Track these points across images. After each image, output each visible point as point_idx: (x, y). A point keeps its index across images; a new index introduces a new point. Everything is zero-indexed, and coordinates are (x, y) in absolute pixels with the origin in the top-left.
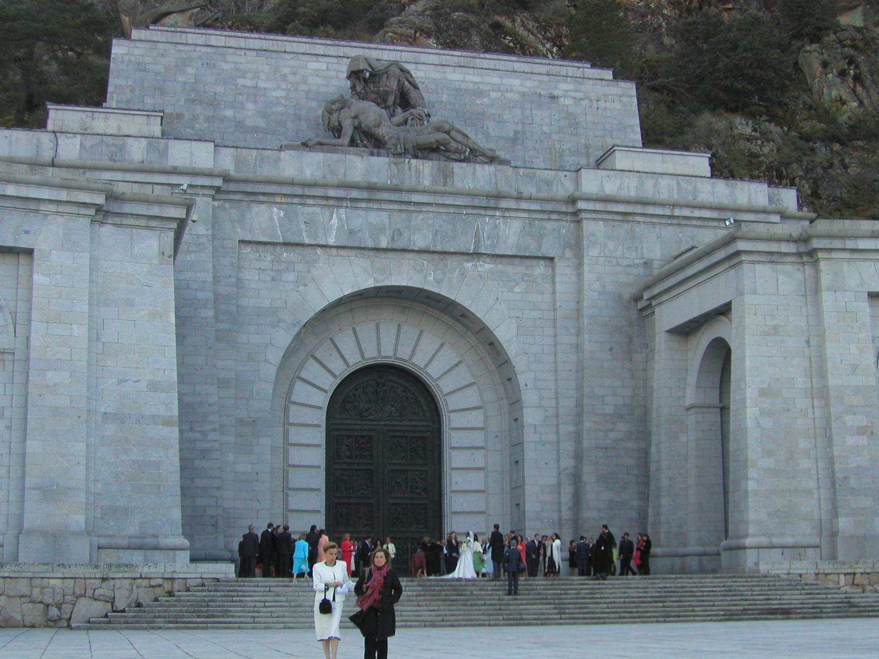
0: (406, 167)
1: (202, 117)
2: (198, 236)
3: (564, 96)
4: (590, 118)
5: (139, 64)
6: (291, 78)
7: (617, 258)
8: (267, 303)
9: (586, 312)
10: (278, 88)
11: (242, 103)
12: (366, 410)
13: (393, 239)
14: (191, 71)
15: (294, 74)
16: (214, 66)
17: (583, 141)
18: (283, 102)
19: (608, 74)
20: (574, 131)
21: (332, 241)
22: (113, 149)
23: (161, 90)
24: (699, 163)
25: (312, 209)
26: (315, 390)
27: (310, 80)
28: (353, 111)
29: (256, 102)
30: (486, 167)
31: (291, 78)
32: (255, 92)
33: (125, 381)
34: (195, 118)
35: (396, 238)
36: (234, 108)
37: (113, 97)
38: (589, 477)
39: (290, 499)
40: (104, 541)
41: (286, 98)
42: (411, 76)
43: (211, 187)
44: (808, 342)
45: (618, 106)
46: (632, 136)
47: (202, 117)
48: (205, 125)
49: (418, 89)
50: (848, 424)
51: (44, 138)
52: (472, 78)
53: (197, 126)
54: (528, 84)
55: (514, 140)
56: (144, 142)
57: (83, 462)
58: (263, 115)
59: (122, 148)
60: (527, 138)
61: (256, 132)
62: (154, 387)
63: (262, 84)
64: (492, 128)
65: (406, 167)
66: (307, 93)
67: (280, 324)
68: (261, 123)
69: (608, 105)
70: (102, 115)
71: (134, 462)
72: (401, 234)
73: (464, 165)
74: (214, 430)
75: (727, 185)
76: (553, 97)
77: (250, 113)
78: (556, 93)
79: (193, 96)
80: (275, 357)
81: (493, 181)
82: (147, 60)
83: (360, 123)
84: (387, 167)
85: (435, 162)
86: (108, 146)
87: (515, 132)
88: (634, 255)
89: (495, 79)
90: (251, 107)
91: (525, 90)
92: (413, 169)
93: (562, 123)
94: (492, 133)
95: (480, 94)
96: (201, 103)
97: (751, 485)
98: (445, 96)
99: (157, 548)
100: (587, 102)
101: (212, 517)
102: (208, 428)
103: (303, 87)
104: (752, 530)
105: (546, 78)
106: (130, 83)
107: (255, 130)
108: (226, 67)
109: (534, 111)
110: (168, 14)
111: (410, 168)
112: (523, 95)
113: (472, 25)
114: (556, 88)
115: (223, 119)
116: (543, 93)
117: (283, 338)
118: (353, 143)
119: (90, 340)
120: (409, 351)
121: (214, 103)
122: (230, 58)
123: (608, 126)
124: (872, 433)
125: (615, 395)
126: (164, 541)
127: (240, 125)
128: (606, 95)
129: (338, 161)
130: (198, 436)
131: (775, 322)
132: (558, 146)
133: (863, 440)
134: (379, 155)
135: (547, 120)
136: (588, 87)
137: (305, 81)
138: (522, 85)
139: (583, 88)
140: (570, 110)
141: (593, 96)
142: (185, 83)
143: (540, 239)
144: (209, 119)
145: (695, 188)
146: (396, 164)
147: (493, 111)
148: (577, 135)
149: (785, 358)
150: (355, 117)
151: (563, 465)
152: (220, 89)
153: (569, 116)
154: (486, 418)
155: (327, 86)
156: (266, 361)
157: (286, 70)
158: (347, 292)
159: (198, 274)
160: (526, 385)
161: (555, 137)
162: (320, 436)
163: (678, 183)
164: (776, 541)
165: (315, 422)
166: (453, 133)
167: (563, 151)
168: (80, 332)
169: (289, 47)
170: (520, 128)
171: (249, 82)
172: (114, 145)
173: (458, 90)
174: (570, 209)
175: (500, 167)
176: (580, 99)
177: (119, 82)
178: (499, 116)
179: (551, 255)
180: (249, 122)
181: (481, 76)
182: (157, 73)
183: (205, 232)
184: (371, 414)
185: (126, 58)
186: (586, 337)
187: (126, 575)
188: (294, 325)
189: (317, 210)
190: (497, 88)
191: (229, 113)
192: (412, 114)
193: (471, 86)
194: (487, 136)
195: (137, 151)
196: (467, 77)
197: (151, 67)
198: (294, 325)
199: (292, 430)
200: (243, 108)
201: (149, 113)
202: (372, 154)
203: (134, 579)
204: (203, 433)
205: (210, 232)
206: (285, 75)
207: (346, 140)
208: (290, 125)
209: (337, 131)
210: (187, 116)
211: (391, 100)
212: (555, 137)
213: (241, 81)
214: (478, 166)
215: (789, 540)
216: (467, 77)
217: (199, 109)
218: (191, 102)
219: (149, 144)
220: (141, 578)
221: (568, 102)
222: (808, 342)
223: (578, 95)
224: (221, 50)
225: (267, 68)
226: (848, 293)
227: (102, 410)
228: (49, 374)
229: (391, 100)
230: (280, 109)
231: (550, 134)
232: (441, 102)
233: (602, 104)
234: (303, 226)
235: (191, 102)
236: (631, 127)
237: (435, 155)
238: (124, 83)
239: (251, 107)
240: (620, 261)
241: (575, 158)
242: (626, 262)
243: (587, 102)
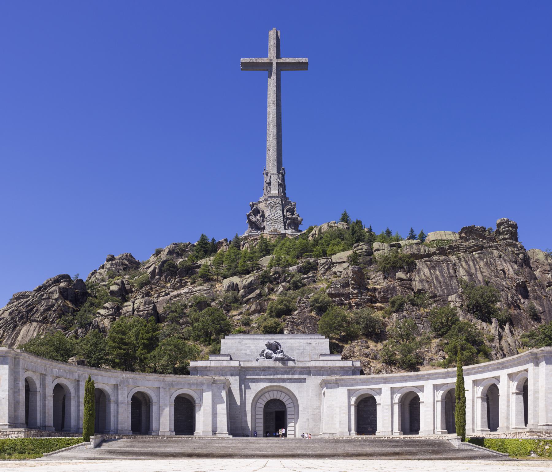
19: (324, 337)
23: (231, 348)
24: (339, 358)
28: (266, 352)
34: (237, 353)
37: (222, 352)
51: (209, 362)
55: (302, 353)
58: (251, 352)
59: (222, 363)
68: (250, 353)
76: (310, 343)
77: (248, 352)
89: (298, 341)
90: (248, 350)
93: (312, 349)
100: (318, 344)
107: (249, 355)
115: (243, 353)
121: (241, 350)
127: (246, 354)
136: (318, 341)
144: (240, 353)
150: (266, 353)
169: (256, 337)
171: (248, 346)
180: (248, 353)
189: (259, 371)
191: (244, 352)
195: (225, 364)
201: (227, 355)
209: (263, 355)
210: (236, 353)
212: (311, 352)
213: (246, 345)
217: (238, 351)
230: (254, 350)
233: (321, 344)
236: (327, 348)
239: (248, 350)
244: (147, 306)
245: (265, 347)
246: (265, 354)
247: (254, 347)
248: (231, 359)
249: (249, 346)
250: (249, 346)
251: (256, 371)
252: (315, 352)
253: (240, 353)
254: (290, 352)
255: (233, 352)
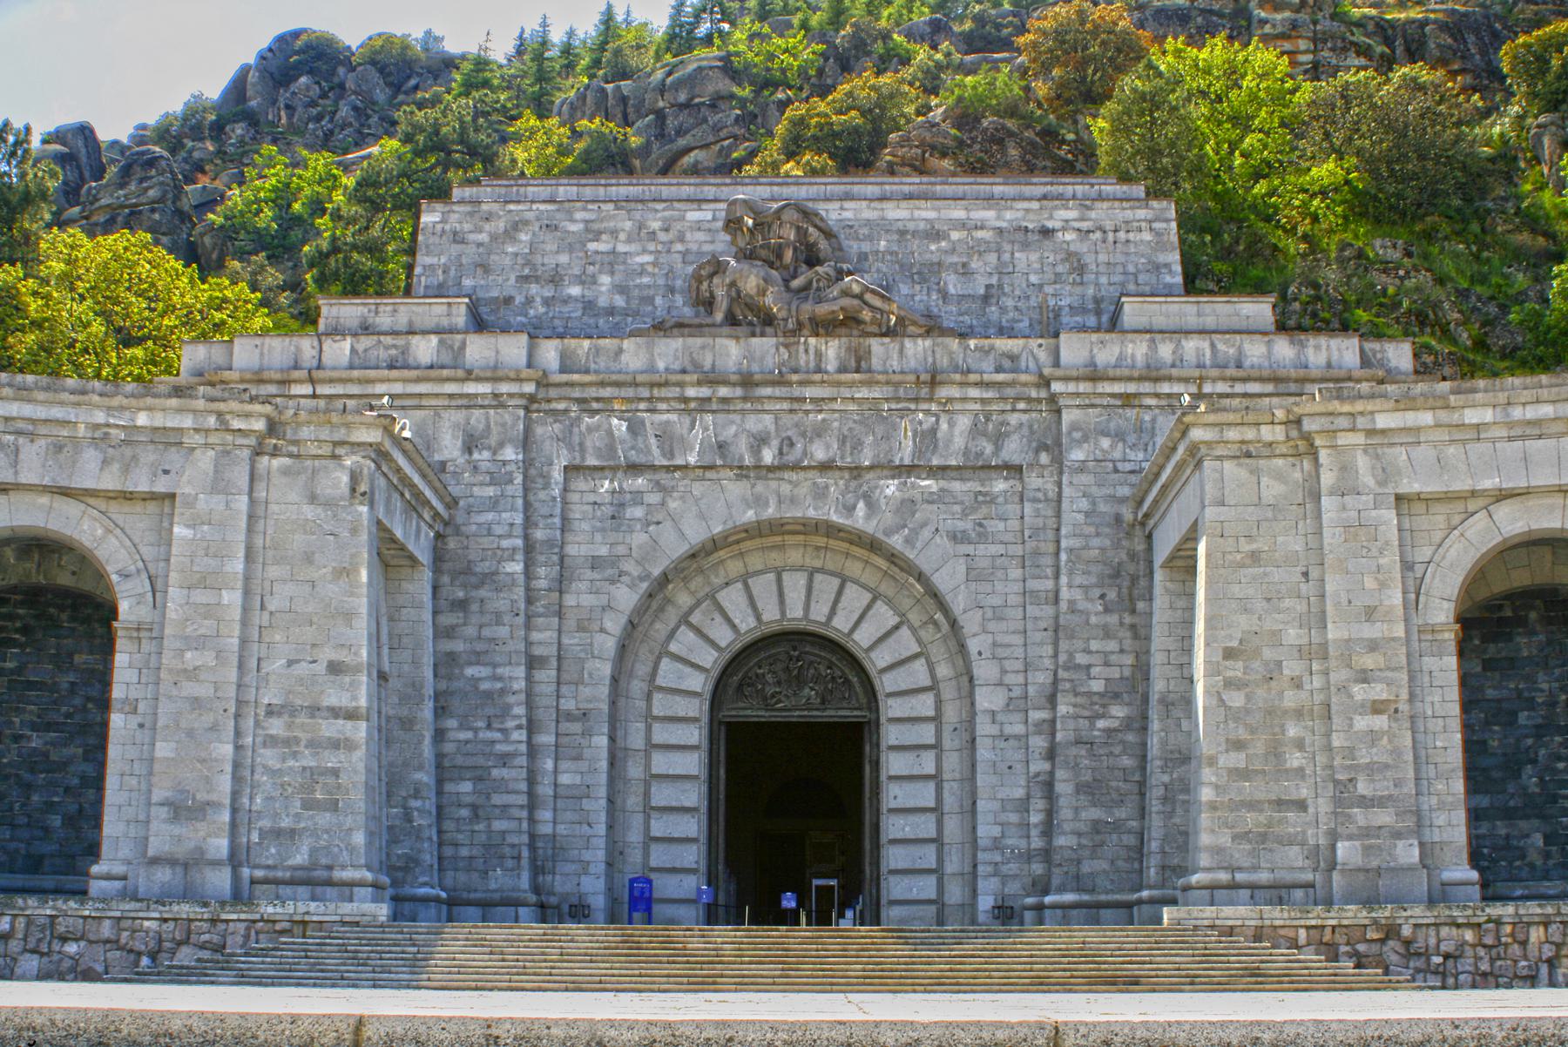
0: (802, 348)
1: (538, 299)
2: (505, 463)
3: (1064, 229)
4: (1102, 258)
5: (455, 233)
6: (662, 236)
7: (1113, 461)
8: (603, 551)
9: (1064, 544)
10: (644, 251)
11: (593, 276)
12: (773, 696)
13: (781, 453)
14: (524, 237)
15: (667, 230)
16: (556, 227)
17: (1091, 291)
18: (650, 269)
20: (1078, 279)
21: (692, 459)
22: (393, 352)
23: (485, 268)
25: (665, 417)
26: (688, 670)
27: (688, 236)
29: (612, 273)
30: (920, 341)
31: (662, 236)
32: (612, 260)
33: (298, 661)
34: (529, 301)
35: (785, 449)
36: (582, 283)
38: (1063, 788)
39: (653, 822)
40: (259, 873)
41: (655, 264)
42: (822, 219)
43: (522, 395)
44: (1306, 574)
45: (1147, 236)
46: (1168, 279)
47: (538, 299)
48: (542, 310)
49: (835, 237)
50: (1358, 698)
52: (926, 213)
53: (532, 312)
54: (1008, 215)
55: (986, 298)
56: (434, 339)
57: (228, 768)
58: (622, 289)
60: (1004, 294)
61: (612, 314)
62: (335, 668)
63: (621, 248)
64: (953, 284)
65: (802, 348)
66: (685, 254)
67: (623, 579)
68: (619, 301)
69: (1131, 236)
70: (389, 308)
71: (304, 768)
72: (792, 445)
73: (887, 340)
74: (519, 727)
75: (1292, 342)
76: (1046, 233)
78: (1050, 224)
79: (527, 271)
80: (614, 625)
81: (930, 360)
82: (467, 227)
83: (739, 292)
84: (773, 350)
85: (844, 340)
86: (387, 348)
87: (988, 287)
88: (1141, 456)
89: (959, 213)
90: (605, 280)
91: (1004, 225)
92: (812, 351)
93: (1060, 269)
94: (952, 290)
95: (935, 234)
96: (537, 279)
97: (1206, 794)
98: (883, 243)
99: (330, 883)
100: (1098, 235)
101: (513, 846)
102: (511, 724)
103: (679, 247)
104: (1204, 860)
105: (1035, 205)
106: (443, 260)
107: (611, 311)
108: (574, 228)
109: (1017, 255)
110: (688, 150)
111: (806, 351)
112: (1000, 231)
113: (1011, 134)
114: (1051, 217)
115: (567, 300)
116: (1031, 226)
117: (626, 598)
118: (732, 320)
119: (246, 609)
120: (826, 610)
121: (555, 279)
122: (579, 215)
123: (1131, 269)
124: (1396, 711)
125: (1107, 664)
126: (339, 874)
127: (589, 305)
128: (1127, 222)
129: (703, 347)
130: (498, 736)
131: (1254, 546)
132: (1052, 302)
133: (1381, 722)
134: (763, 335)
135: (1037, 266)
136: (1100, 212)
137: (681, 239)
138: (998, 218)
139: (1093, 214)
140: (1072, 248)
141: (1109, 225)
142: (516, 255)
143: (999, 439)
144: (547, 302)
145: (1240, 350)
146: (786, 346)
147: (955, 259)
148: (1082, 283)
149: (1268, 600)
151: (1033, 768)
152: (564, 259)
153: (1070, 255)
154: (939, 703)
155: (712, 242)
156: (602, 630)
157: (656, 225)
158: (718, 529)
159: (504, 515)
160: (980, 653)
161: (1049, 289)
162: (694, 735)
163: (1213, 345)
164: (1240, 877)
165: (691, 714)
166: (868, 297)
167: (1060, 308)
168: (232, 598)
169: (666, 192)
170: (994, 280)
172: (395, 346)
173: (902, 233)
174: (1043, 394)
175: (940, 340)
176: (1089, 232)
177: (428, 260)
178: (964, 265)
179: (1017, 462)
180: (603, 302)
181: (938, 209)
182: (480, 245)
183: (513, 457)
184: (780, 701)
185: (439, 227)
186: (1064, 580)
187: (243, 916)
188: (641, 579)
189: (673, 417)
190: (962, 225)
191: (575, 291)
192: (817, 273)
193: (922, 226)
194: (944, 295)
196: (917, 213)
197: (472, 237)
198: (641, 579)
199: (656, 727)
200: (595, 283)
202: (753, 335)
203: (254, 921)
204: (504, 731)
205: (520, 457)
206: (654, 233)
207: (719, 316)
208: (658, 301)
210: (519, 299)
211: (789, 255)
212: (1049, 289)
213: (592, 246)
214: (908, 343)
215: (1263, 877)
216: (917, 213)
217: (534, 288)
218: (524, 279)
219: (441, 342)
220: (262, 920)
221: (1070, 236)
222: (1306, 574)
223: (1085, 225)
224: (567, 205)
225: (628, 225)
226: (1364, 498)
227: (266, 701)
228: (189, 655)
229: (789, 255)
230: (646, 280)
231: (1041, 286)
232: (877, 252)
233: (1122, 235)
234: (653, 441)
235: (524, 279)
236: (1167, 265)
237: (843, 330)
238: (435, 260)
239: (605, 280)
240: (1120, 466)
241: (1078, 319)
242: (1128, 467)
243: (1098, 235)
244: (133, 187)
245: (721, 243)
246: (720, 293)
247: (647, 258)
248: (479, 324)
249: (613, 252)
250: (613, 252)
251: (652, 411)
252: (1078, 290)
253: (547, 302)
254: (905, 289)
255: (495, 293)
